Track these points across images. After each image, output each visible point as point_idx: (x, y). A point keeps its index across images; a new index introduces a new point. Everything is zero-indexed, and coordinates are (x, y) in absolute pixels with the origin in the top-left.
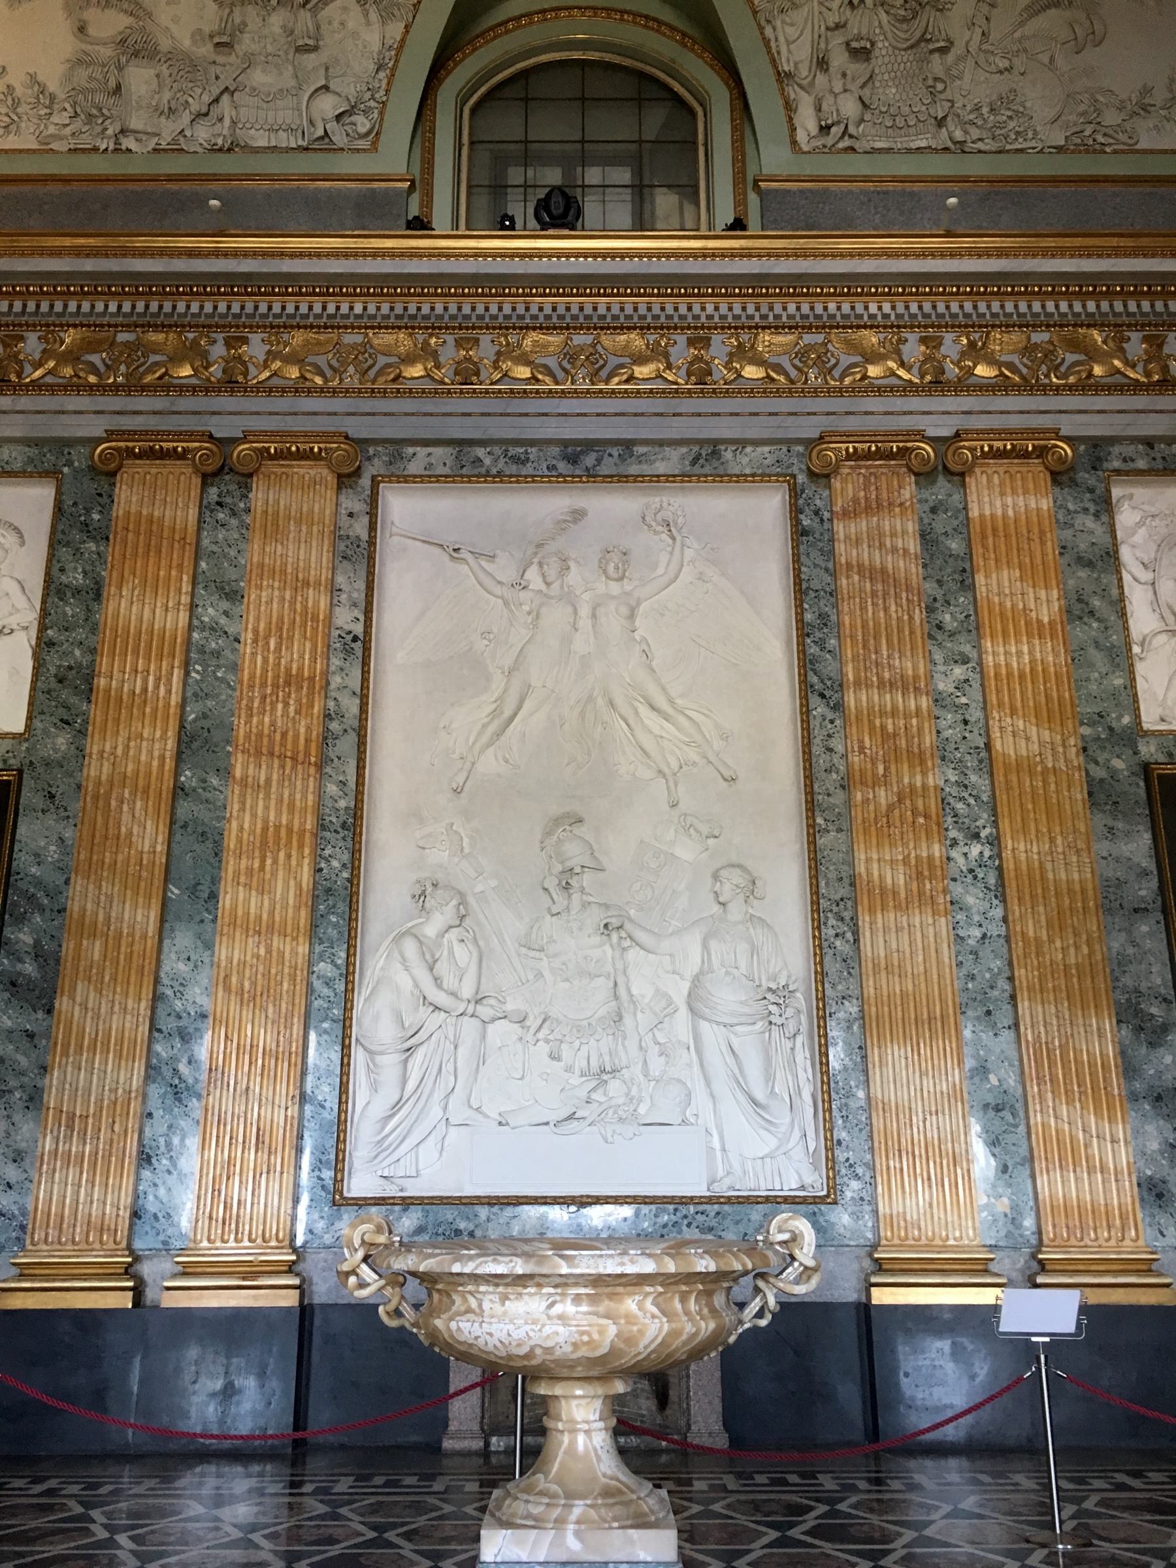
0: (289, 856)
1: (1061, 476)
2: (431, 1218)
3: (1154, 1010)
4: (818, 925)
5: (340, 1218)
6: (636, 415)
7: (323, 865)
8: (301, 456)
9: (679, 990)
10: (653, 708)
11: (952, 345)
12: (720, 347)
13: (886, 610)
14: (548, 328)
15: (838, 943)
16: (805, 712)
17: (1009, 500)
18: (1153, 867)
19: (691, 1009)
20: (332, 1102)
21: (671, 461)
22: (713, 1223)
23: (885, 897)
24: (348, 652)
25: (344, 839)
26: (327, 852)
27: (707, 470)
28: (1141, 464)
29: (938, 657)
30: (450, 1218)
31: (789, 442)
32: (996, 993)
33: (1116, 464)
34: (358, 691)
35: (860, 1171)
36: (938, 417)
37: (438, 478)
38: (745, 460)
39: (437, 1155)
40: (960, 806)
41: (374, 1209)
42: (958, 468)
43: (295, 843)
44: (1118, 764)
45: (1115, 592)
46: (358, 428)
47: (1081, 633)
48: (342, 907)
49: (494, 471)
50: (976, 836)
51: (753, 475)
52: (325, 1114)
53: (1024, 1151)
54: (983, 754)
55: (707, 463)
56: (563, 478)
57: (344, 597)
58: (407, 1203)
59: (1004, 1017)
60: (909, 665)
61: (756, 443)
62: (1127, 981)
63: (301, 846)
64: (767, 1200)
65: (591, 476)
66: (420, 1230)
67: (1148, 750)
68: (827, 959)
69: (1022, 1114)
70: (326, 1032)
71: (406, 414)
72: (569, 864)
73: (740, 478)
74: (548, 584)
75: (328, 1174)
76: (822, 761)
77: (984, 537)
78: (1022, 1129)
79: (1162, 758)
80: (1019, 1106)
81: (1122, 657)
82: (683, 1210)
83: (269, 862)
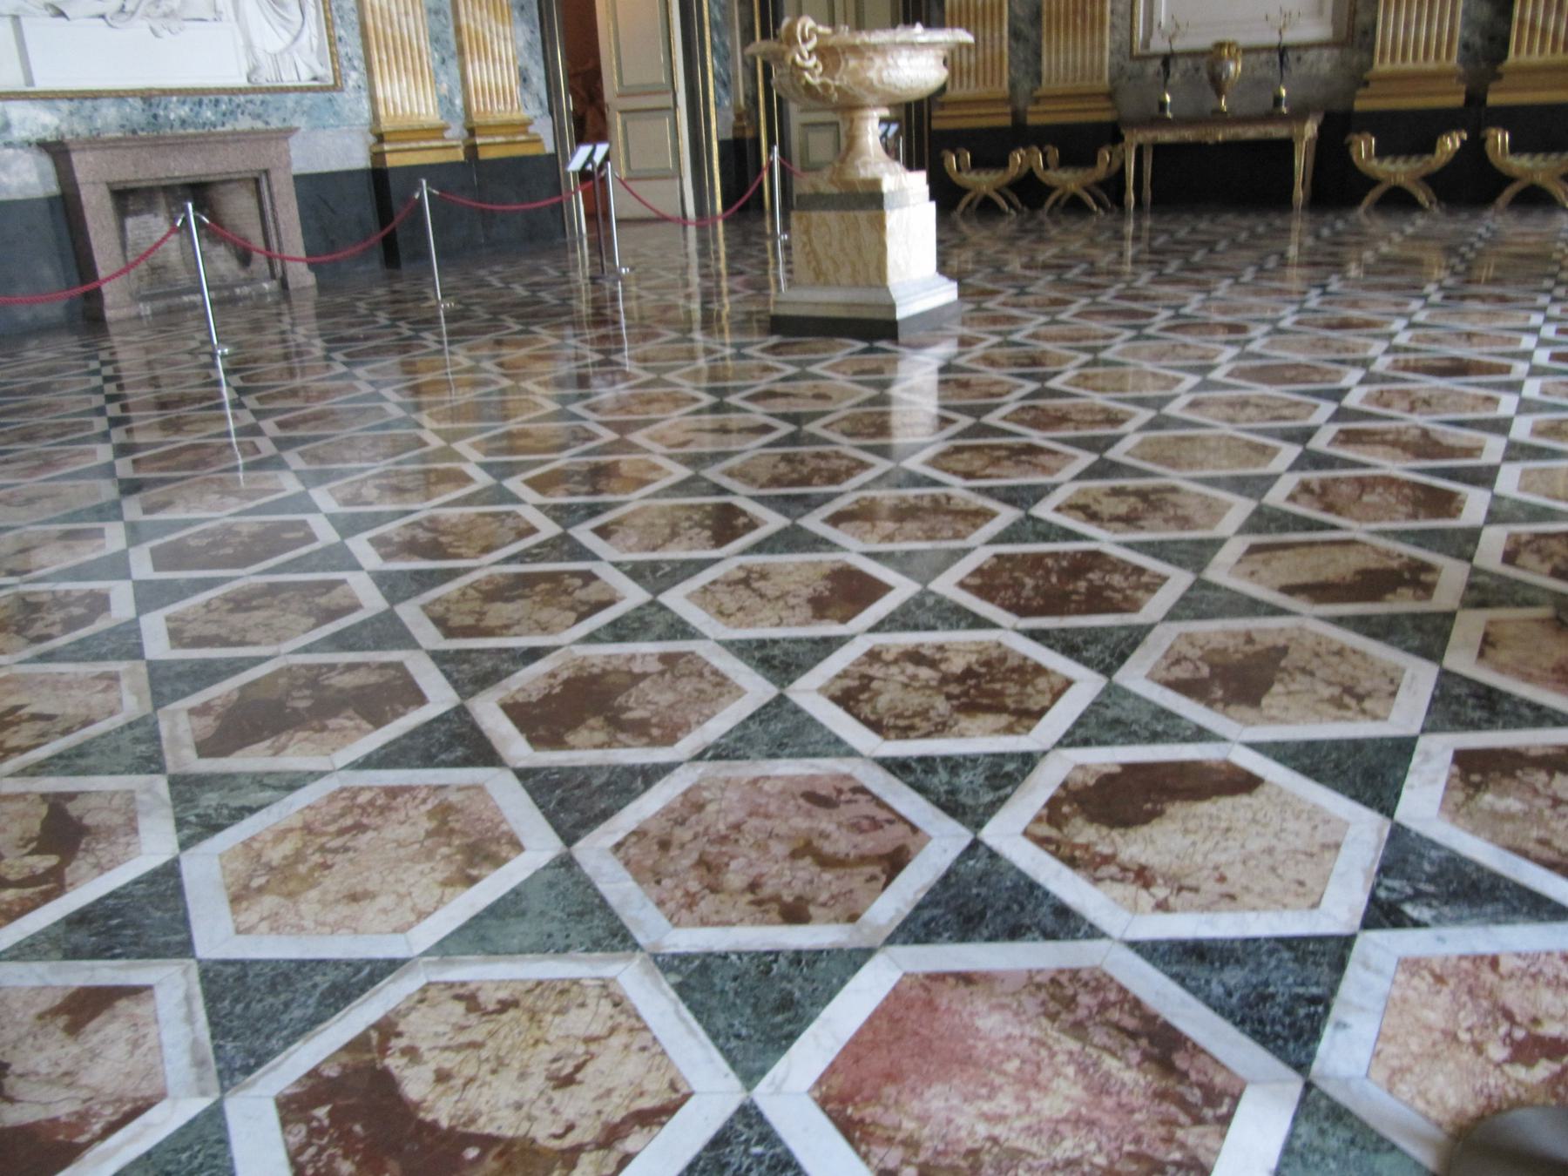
22: (260, 110)
35: (356, 63)
53: (453, 47)
64: (296, 89)
78: (451, 30)
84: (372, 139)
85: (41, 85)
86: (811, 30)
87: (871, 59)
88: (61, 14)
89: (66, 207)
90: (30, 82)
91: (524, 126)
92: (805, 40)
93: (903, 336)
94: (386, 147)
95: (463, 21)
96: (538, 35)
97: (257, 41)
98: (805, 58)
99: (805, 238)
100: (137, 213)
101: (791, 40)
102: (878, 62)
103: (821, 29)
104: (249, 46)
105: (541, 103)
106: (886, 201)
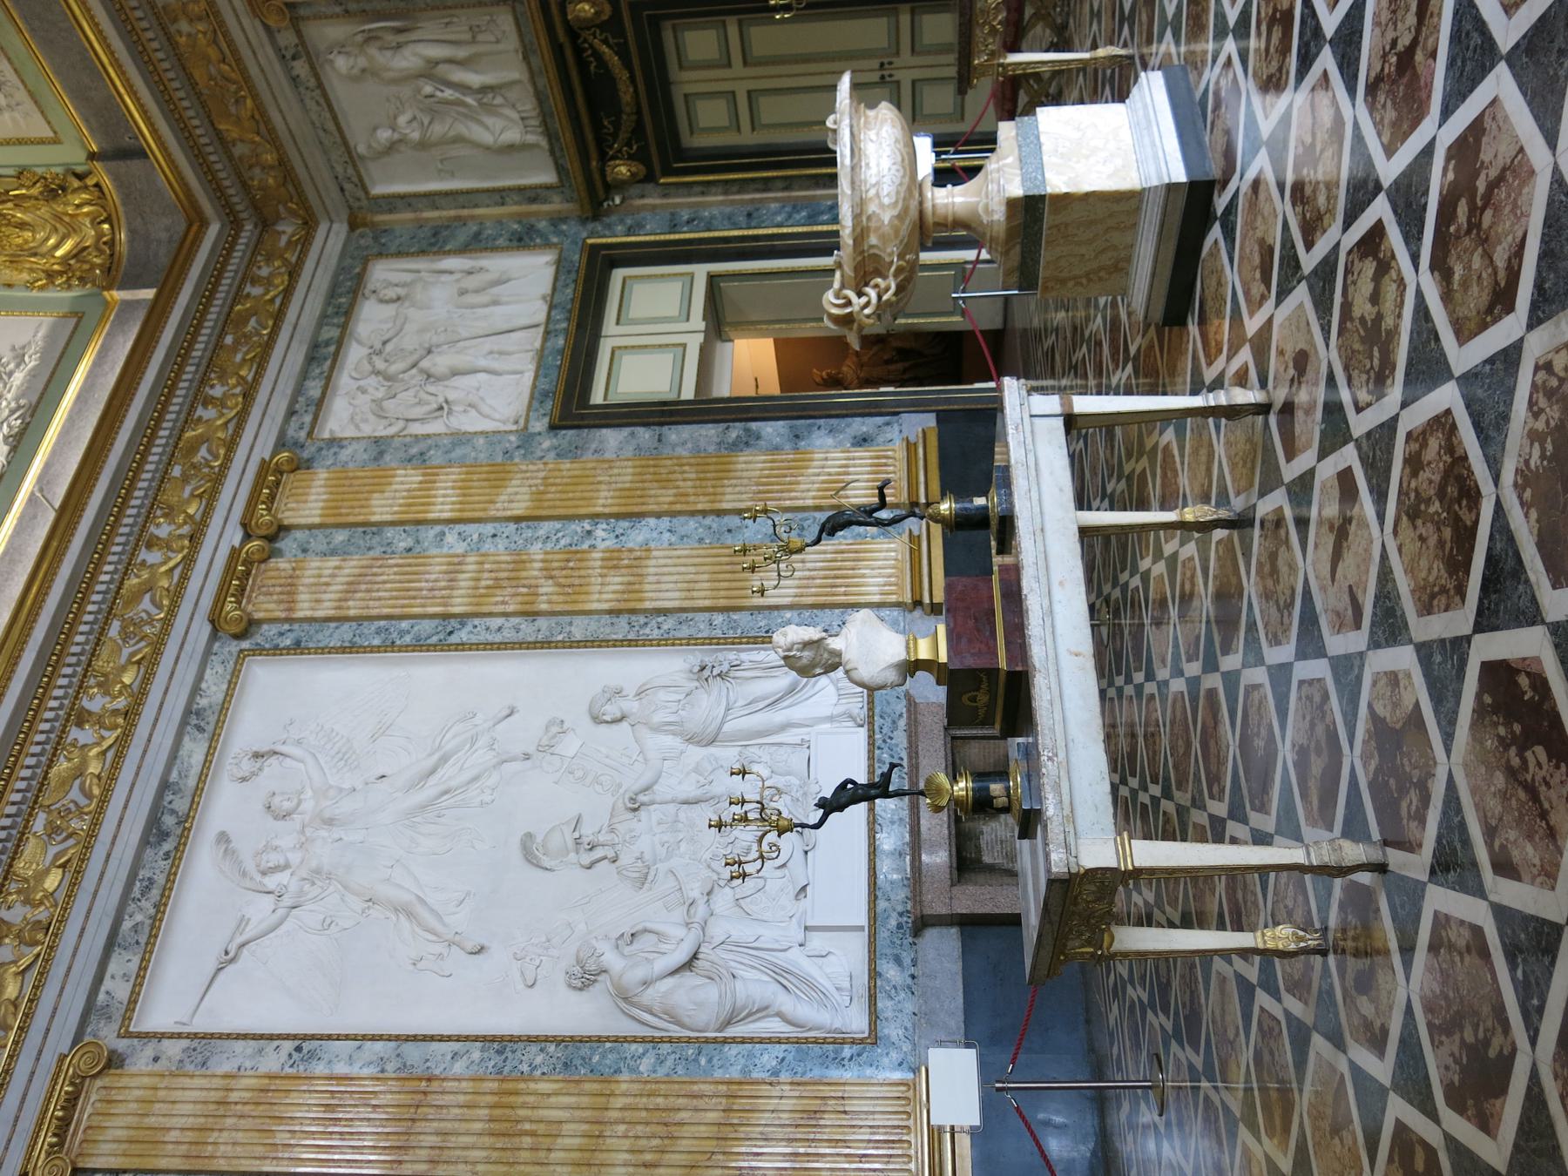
0: (524, 1106)
1: (301, 465)
2: (888, 951)
3: (734, 435)
4: (648, 643)
5: (888, 1037)
6: (137, 774)
7: (538, 1073)
8: (71, 1102)
9: (696, 753)
10: (432, 772)
11: (163, 530)
12: (95, 703)
13: (385, 582)
14: (16, 853)
15: (665, 627)
16: (461, 647)
17: (313, 498)
18: (626, 431)
19: (711, 742)
20: (779, 1050)
21: (194, 751)
23: (632, 589)
24: (312, 1055)
25: (514, 1052)
26: (525, 1068)
27: (213, 719)
28: (308, 419)
29: (434, 551)
30: (887, 934)
31: (208, 652)
32: (715, 526)
33: (303, 434)
34: (358, 1043)
36: (224, 536)
37: (143, 968)
38: (214, 688)
39: (830, 957)
40: (563, 542)
41: (879, 1005)
42: (275, 528)
43: (512, 1099)
44: (546, 444)
45: (408, 439)
46: (61, 1040)
47: (436, 457)
48: (585, 1050)
49: (152, 911)
50: (589, 533)
51: (230, 682)
52: (790, 1057)
54: (523, 525)
55: (205, 721)
56: (180, 847)
57: (248, 1064)
58: (874, 974)
59: (734, 521)
60: (436, 569)
61: (200, 677)
62: (711, 449)
63: (516, 1093)
65: (186, 822)
66: (898, 960)
67: (539, 425)
68: (678, 635)
69: (806, 515)
70: (710, 1061)
71: (60, 995)
72: (570, 844)
73: (229, 694)
74: (287, 866)
75: (847, 1051)
76: (508, 635)
77: (340, 515)
79: (546, 420)
80: (800, 515)
81: (461, 438)
82: (879, 743)
83: (527, 1126)
84: (918, 613)
85: (863, 920)
86: (837, 296)
87: (869, 218)
88: (804, 888)
89: (969, 924)
90: (861, 928)
91: (910, 447)
92: (849, 303)
93: (1215, 171)
94: (926, 600)
95: (810, 502)
96: (822, 422)
97: (827, 712)
98: (865, 303)
99: (1070, 284)
100: (978, 849)
101: (847, 320)
102: (872, 208)
103: (836, 285)
104: (831, 719)
105: (888, 424)
106: (1036, 192)
